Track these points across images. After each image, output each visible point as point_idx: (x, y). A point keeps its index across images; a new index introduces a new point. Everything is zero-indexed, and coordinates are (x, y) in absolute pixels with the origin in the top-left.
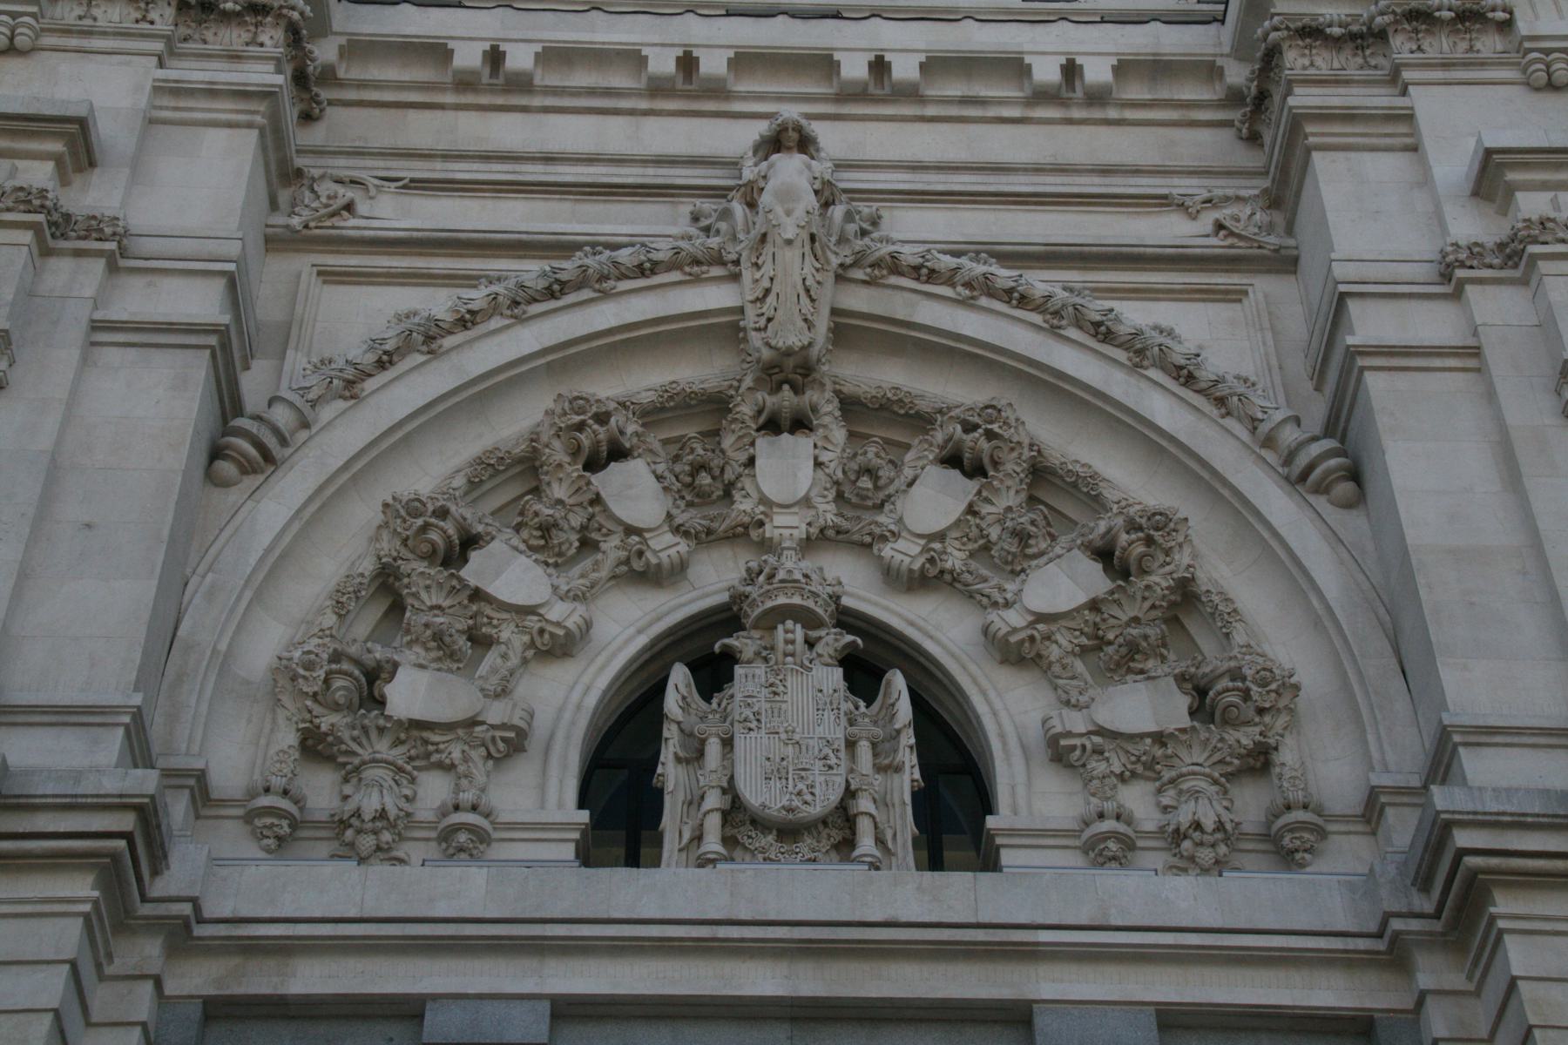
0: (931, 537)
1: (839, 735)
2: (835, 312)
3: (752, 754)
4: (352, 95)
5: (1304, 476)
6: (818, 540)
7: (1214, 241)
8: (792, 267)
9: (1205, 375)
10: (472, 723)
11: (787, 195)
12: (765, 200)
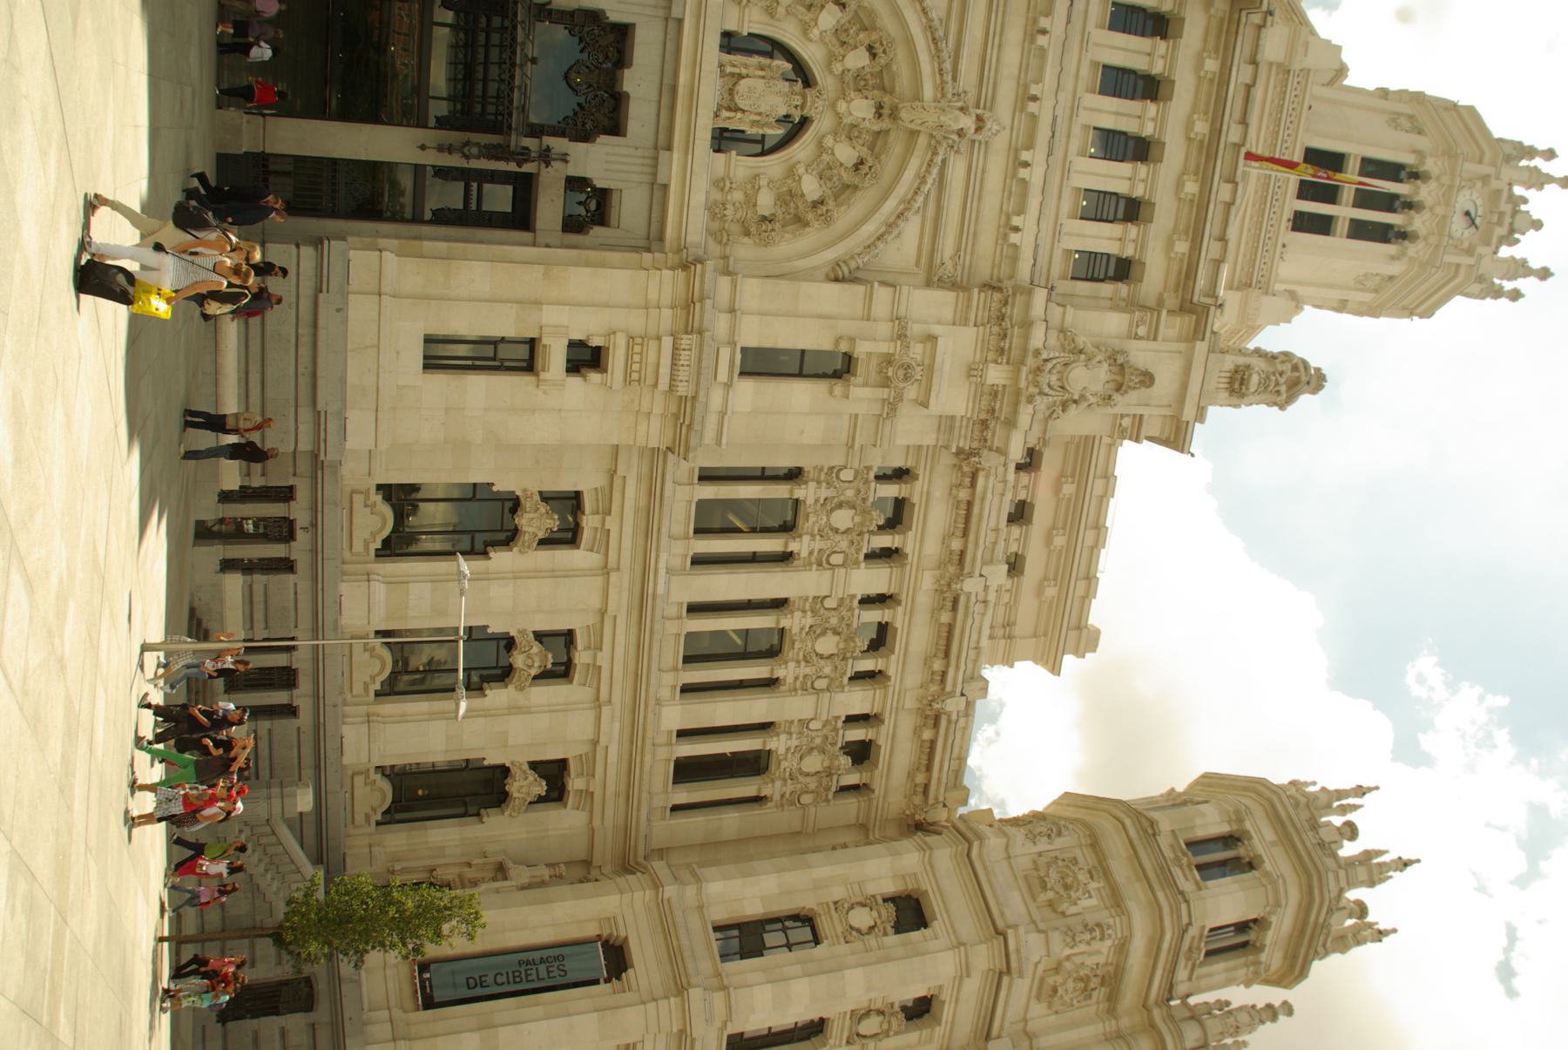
0: (832, 150)
1: (762, 110)
2: (919, 132)
5: (838, 265)
6: (839, 116)
8: (932, 118)
9: (881, 245)
11: (956, 120)
12: (957, 112)
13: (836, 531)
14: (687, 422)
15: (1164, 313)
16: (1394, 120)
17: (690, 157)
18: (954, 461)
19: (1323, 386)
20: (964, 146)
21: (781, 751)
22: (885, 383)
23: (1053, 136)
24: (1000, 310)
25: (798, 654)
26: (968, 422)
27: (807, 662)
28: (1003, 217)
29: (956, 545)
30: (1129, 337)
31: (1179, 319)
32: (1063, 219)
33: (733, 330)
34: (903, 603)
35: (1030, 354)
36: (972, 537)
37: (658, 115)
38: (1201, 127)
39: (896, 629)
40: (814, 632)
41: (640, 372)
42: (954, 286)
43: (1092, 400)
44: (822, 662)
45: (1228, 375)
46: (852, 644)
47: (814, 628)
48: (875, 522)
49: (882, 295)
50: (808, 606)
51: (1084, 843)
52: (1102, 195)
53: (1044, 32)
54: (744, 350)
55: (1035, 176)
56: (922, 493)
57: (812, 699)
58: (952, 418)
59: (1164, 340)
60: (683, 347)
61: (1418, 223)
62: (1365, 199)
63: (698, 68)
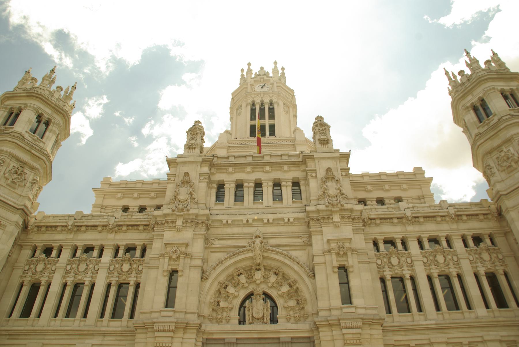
0: (272, 283)
2: (263, 256)
3: (254, 310)
4: (212, 227)
5: (309, 276)
6: (261, 282)
7: (303, 243)
8: (258, 252)
9: (300, 264)
10: (228, 307)
11: (257, 244)
12: (255, 244)
13: (399, 262)
14: (371, 321)
15: (307, 169)
16: (239, 114)
17: (281, 331)
18: (367, 227)
19: (320, 116)
20: (265, 241)
21: (484, 269)
22: (346, 254)
23: (258, 213)
24: (315, 221)
25: (446, 268)
26: (354, 224)
27: (448, 265)
28: (286, 225)
29: (396, 221)
30: (317, 178)
31: (308, 164)
32: (283, 206)
33: (337, 309)
34: (420, 235)
35: (328, 208)
36: (392, 216)
37: (268, 343)
38: (249, 169)
39: (429, 236)
40: (437, 264)
41: (356, 340)
42: (310, 237)
43: (339, 186)
44: (447, 259)
45: (323, 145)
46: (438, 250)
47: (435, 264)
48: (394, 250)
49: (317, 260)
50: (428, 268)
51: (490, 157)
52: (274, 195)
53: (227, 221)
54: (343, 304)
55: (271, 217)
56: (380, 235)
57: (461, 261)
58: (353, 230)
59: (316, 167)
60: (345, 325)
61: (267, 100)
62: (262, 117)
63: (251, 331)
